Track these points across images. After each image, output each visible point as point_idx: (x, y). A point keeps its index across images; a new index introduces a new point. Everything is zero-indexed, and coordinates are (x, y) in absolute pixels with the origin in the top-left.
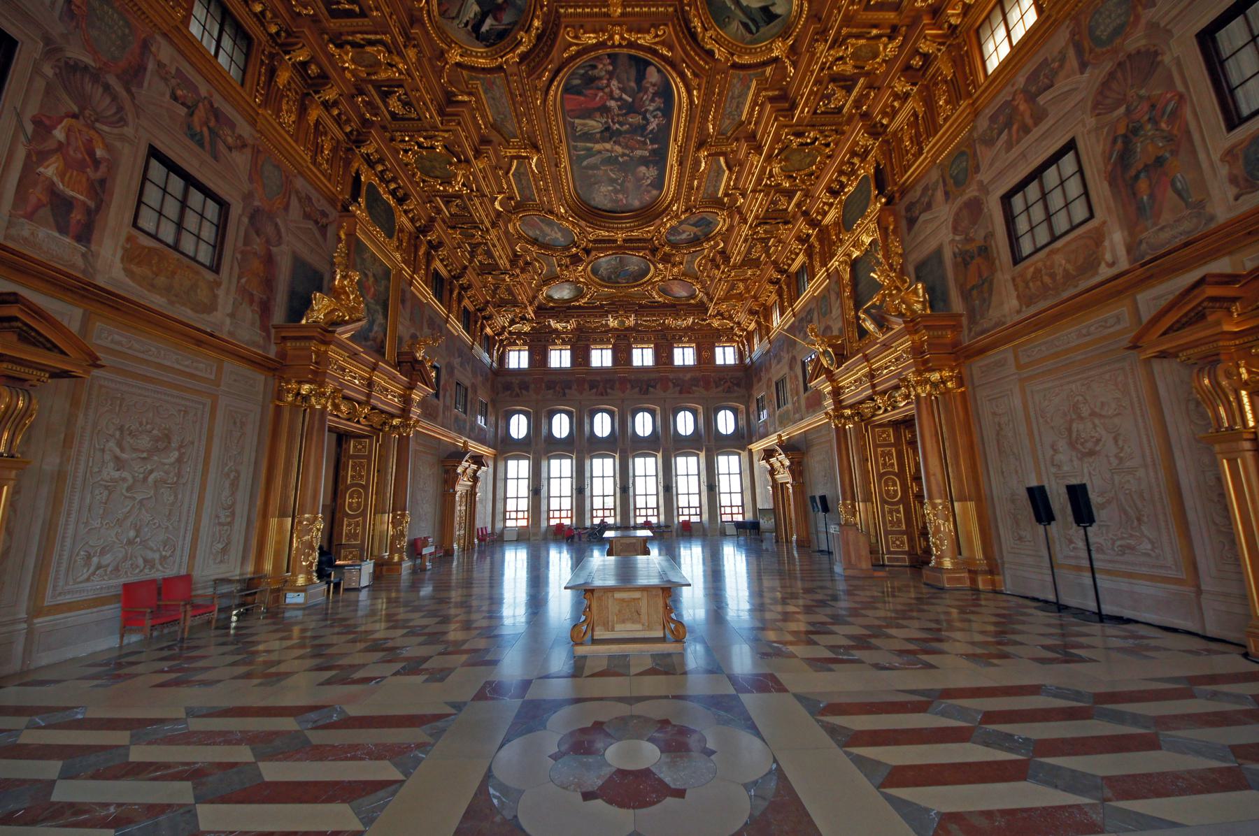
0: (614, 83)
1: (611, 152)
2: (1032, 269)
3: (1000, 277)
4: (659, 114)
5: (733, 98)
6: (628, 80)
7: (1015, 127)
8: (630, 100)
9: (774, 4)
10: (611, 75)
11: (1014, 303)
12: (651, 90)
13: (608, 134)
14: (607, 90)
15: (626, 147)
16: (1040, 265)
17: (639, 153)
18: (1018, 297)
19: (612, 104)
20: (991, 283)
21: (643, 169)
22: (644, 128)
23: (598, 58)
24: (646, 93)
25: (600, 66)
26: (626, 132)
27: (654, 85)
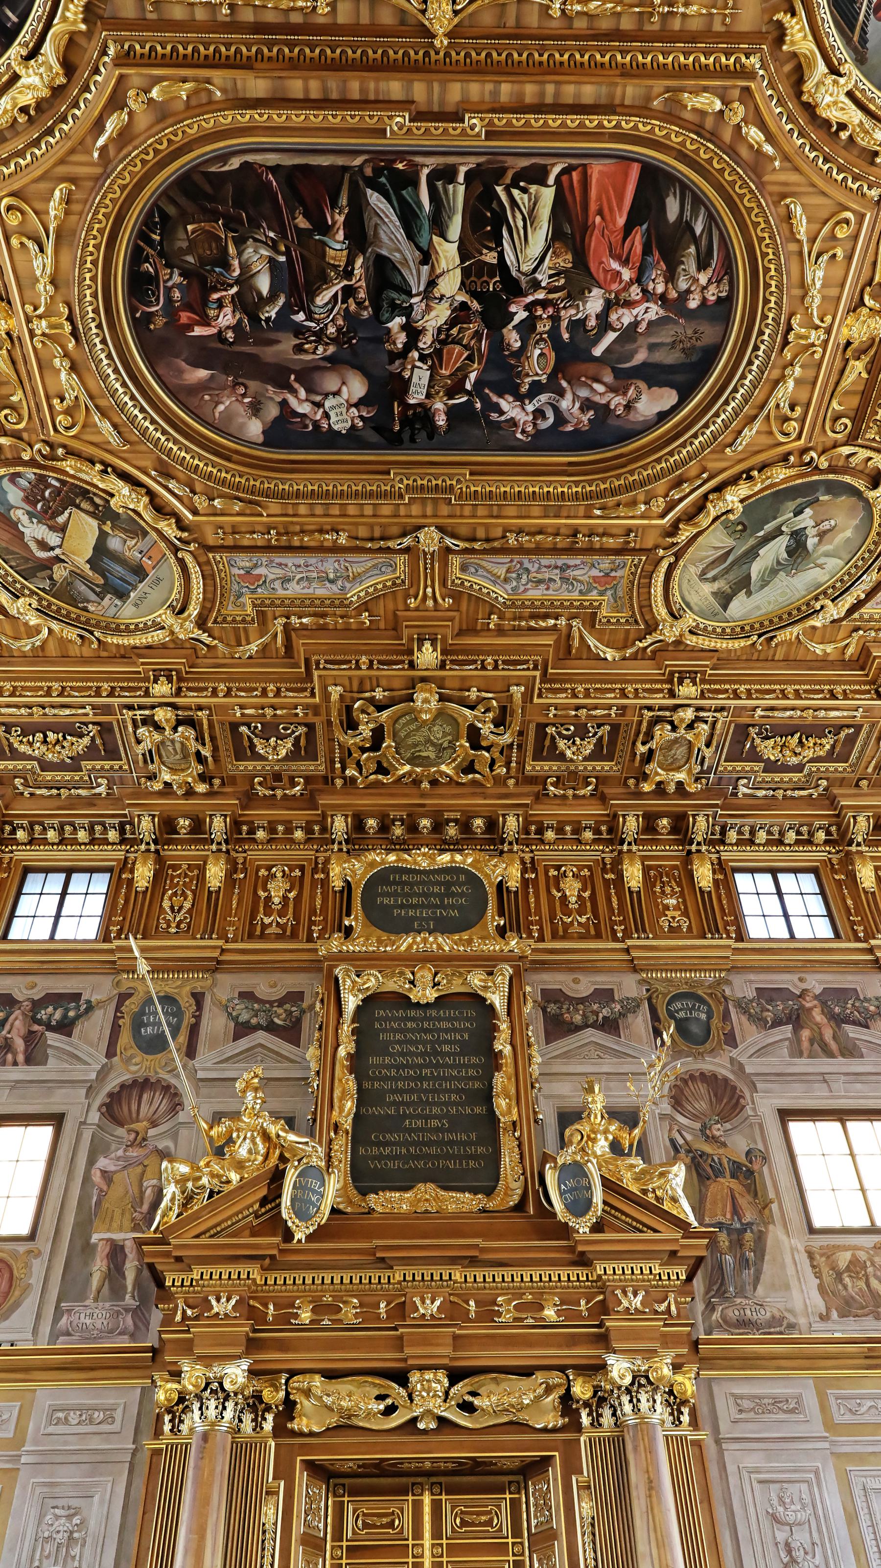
0: (654, 311)
1: (428, 293)
2: (847, 1256)
3: (776, 1234)
4: (544, 425)
5: (563, 568)
6: (652, 347)
7: (805, 1034)
8: (598, 351)
9: (749, 594)
10: (675, 305)
11: (818, 1302)
12: (617, 401)
13: (493, 291)
14: (635, 292)
15: (444, 338)
16: (862, 1256)
17: (421, 377)
18: (821, 1289)
19: (594, 304)
20: (760, 1238)
21: (357, 387)
22: (510, 388)
23: (728, 268)
24: (611, 389)
25: (703, 278)
26: (498, 344)
27: (628, 407)
